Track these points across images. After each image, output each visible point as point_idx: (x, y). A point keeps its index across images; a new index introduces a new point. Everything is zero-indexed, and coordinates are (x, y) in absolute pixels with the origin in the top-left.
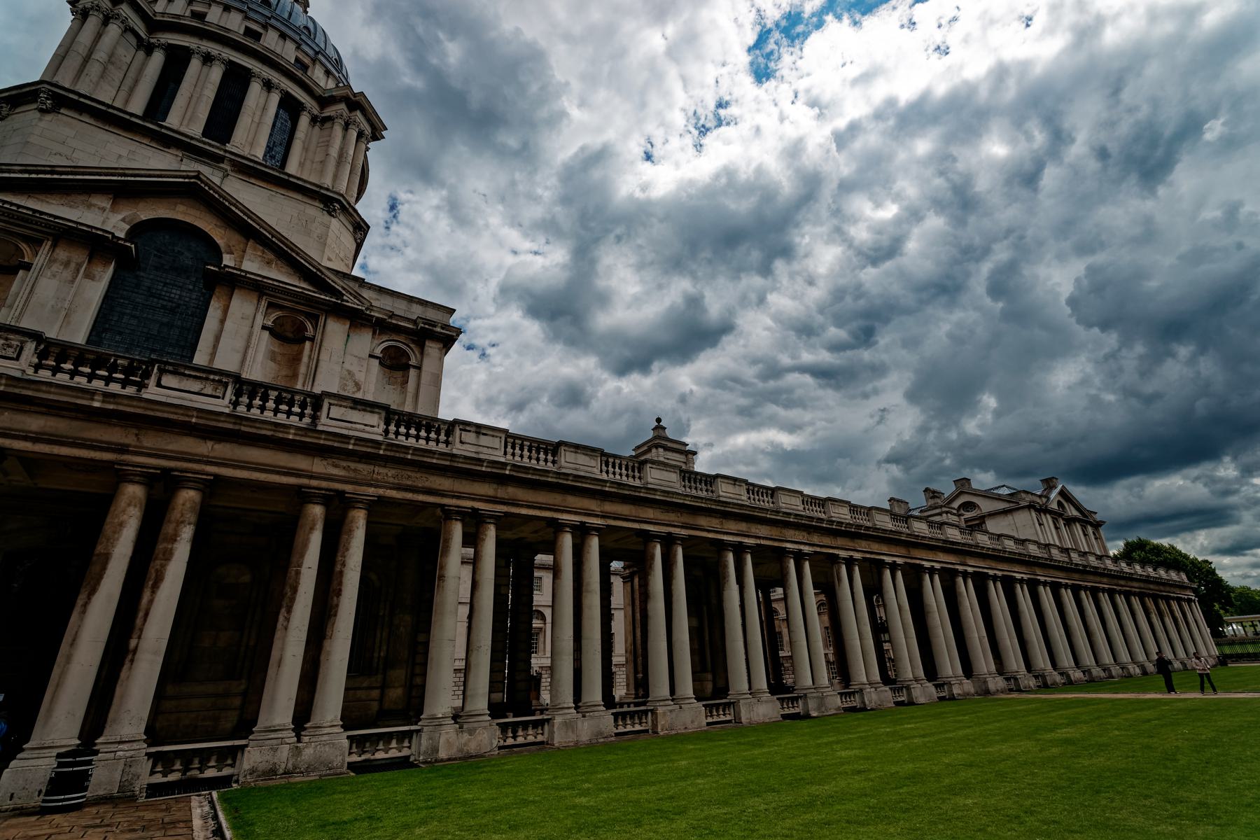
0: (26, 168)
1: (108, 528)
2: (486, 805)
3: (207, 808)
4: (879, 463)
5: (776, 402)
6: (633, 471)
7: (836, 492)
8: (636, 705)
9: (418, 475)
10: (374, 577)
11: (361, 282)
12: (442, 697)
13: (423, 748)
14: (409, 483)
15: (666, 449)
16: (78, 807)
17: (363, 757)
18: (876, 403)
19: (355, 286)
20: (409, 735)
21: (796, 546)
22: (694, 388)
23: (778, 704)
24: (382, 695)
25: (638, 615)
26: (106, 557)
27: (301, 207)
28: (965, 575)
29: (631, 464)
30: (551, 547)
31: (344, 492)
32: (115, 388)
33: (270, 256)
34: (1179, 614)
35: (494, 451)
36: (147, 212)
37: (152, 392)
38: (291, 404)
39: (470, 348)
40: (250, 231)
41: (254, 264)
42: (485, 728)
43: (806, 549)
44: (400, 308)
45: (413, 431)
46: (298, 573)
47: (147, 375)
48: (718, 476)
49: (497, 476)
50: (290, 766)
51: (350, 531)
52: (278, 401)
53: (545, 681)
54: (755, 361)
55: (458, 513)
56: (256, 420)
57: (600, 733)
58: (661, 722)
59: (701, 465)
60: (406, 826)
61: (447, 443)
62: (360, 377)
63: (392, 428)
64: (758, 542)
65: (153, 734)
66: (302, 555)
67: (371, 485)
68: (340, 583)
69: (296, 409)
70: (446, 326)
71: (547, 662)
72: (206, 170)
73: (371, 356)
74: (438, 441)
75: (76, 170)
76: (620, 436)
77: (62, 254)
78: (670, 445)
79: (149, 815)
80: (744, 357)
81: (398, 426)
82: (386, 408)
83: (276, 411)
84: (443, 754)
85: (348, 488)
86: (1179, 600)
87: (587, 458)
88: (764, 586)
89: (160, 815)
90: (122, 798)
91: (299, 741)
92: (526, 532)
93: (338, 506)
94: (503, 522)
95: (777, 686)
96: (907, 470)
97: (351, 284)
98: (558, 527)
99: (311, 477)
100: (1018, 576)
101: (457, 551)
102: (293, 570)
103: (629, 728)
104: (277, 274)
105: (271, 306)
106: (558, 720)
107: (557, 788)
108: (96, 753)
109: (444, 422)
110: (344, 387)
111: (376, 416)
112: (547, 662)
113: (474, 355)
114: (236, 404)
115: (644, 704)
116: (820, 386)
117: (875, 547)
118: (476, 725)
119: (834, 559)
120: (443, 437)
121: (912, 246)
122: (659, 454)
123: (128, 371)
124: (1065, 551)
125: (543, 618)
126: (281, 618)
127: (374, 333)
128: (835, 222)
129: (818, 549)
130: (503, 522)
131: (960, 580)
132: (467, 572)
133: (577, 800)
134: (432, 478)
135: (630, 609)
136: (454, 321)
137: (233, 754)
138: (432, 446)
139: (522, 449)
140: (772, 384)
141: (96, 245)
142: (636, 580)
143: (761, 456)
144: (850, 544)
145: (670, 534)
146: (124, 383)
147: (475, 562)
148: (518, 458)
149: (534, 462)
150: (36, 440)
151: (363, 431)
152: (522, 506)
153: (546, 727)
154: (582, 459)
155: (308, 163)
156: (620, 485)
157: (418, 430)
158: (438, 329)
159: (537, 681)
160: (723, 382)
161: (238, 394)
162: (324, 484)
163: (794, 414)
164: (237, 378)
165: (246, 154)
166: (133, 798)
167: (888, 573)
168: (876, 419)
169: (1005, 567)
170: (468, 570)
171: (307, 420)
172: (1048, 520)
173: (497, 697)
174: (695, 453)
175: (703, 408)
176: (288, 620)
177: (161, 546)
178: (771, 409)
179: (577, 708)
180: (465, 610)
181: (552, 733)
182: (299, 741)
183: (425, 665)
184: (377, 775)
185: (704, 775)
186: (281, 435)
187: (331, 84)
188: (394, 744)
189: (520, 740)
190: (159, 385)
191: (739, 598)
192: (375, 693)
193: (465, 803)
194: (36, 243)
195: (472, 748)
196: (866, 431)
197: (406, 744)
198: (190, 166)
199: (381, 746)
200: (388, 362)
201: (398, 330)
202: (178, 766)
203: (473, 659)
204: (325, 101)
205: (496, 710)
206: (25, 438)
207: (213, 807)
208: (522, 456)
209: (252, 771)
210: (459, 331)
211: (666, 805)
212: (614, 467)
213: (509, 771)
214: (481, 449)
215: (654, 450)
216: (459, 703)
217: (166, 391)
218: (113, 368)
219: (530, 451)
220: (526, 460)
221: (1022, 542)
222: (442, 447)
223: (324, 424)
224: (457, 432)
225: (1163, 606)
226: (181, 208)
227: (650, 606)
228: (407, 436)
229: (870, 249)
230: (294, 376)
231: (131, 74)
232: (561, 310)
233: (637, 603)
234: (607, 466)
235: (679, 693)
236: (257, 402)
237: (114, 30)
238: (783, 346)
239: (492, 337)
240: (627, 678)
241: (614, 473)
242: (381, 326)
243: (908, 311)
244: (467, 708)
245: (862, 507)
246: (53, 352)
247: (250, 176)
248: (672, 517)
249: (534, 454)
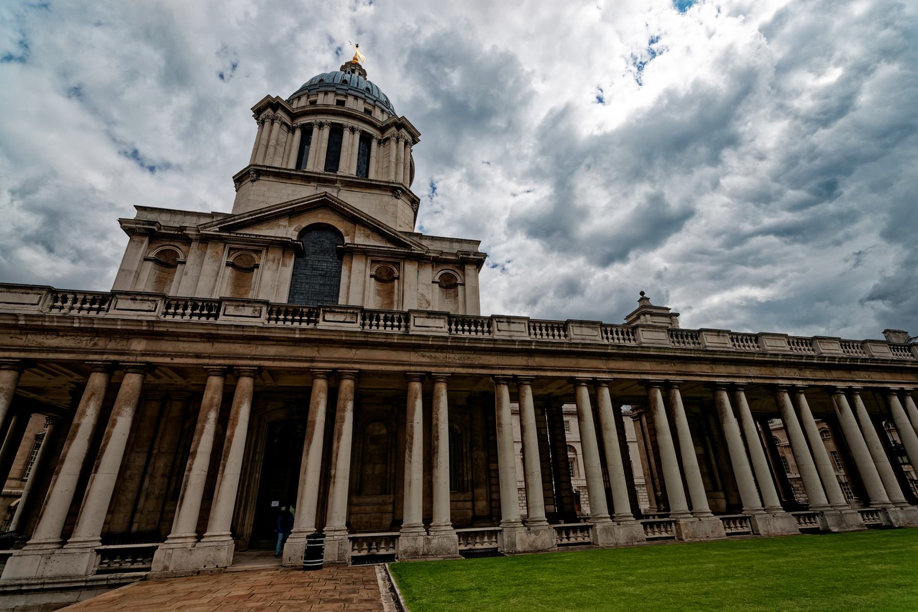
0: (251, 214)
1: (311, 406)
2: (556, 586)
3: (384, 574)
4: (861, 302)
5: (744, 264)
6: (628, 335)
7: (821, 331)
8: (660, 517)
9: (474, 356)
10: (456, 427)
12: (513, 509)
13: (505, 543)
14: (469, 362)
15: (652, 314)
16: (320, 568)
17: (468, 547)
18: (849, 248)
19: (416, 239)
20: (495, 533)
21: (789, 382)
22: (667, 265)
23: (795, 520)
24: (473, 505)
25: (650, 446)
26: (314, 422)
27: (380, 197)
29: (625, 330)
30: (573, 398)
31: (431, 373)
32: (304, 325)
33: (368, 232)
35: (521, 333)
37: (322, 325)
38: (392, 321)
39: (494, 266)
40: (356, 219)
41: (360, 239)
42: (545, 530)
43: (800, 384)
44: (446, 247)
45: (466, 327)
46: (412, 427)
47: (317, 316)
48: (701, 330)
49: (526, 350)
50: (425, 550)
51: (438, 397)
52: (385, 320)
53: (584, 497)
54: (717, 234)
55: (504, 379)
56: (375, 333)
57: (633, 538)
58: (684, 532)
59: (684, 323)
60: (504, 597)
61: (489, 332)
62: (429, 297)
63: (453, 327)
64: (750, 381)
65: (351, 527)
66: (413, 415)
67: (446, 366)
68: (437, 432)
69: (396, 323)
70: (476, 254)
71: (584, 483)
72: (328, 190)
73: (433, 282)
74: (483, 332)
75: (270, 208)
76: (613, 311)
77: (271, 256)
78: (654, 311)
79: (355, 575)
80: (707, 233)
81: (456, 325)
82: (448, 314)
83: (385, 326)
84: (519, 548)
85: (433, 369)
87: (590, 330)
88: (761, 418)
89: (361, 576)
90: (339, 564)
91: (428, 534)
92: (552, 389)
93: (428, 381)
94: (536, 383)
95: (789, 504)
96: (896, 303)
97: (415, 238)
98: (576, 383)
99: (411, 365)
101: (507, 407)
102: (408, 425)
103: (657, 535)
104: (373, 242)
105: (373, 261)
106: (599, 527)
107: (607, 578)
108: (324, 536)
109: (485, 318)
110: (420, 305)
111: (442, 321)
112: (584, 483)
113: (497, 270)
114: (363, 325)
115: (667, 516)
116: (786, 243)
117: (876, 376)
118: (539, 528)
119: (832, 391)
120: (486, 329)
121: (864, 99)
122: (647, 320)
123: (309, 314)
125: (575, 451)
126: (407, 455)
127: (433, 267)
128: (778, 100)
129: (813, 383)
130: (536, 383)
132: (515, 420)
133: (625, 589)
134: (484, 357)
135: (642, 442)
136: (481, 249)
137: (392, 541)
138: (480, 335)
139: (541, 330)
140: (737, 249)
141: (284, 246)
142: (644, 419)
143: (736, 311)
144: (847, 376)
145: (667, 381)
146: (308, 322)
147: (520, 413)
148: (539, 337)
149: (551, 337)
150: (274, 360)
151: (436, 331)
152: (547, 370)
153: (590, 531)
154: (586, 331)
155: (380, 171)
156: (619, 347)
157: (470, 326)
158: (472, 257)
159: (577, 497)
160: (689, 257)
161: (364, 319)
162: (418, 369)
163: (764, 271)
164: (362, 310)
165: (347, 175)
166: (345, 564)
167: (896, 400)
168: (852, 262)
170: (517, 417)
171: (403, 329)
173: (551, 508)
174: (677, 315)
175: (677, 279)
176: (410, 456)
177: (338, 414)
178: (741, 270)
179: (612, 518)
180: (519, 446)
181: (595, 536)
182: (428, 534)
183: (498, 485)
184: (479, 560)
185: (734, 577)
186: (390, 341)
187: (385, 117)
188: (486, 539)
189: (572, 540)
190: (324, 320)
191: (739, 430)
192: (469, 504)
193: (541, 584)
194: (258, 252)
195: (539, 544)
196: (843, 274)
197: (494, 539)
198: (322, 190)
199: (478, 540)
200: (444, 285)
201: (447, 262)
202: (365, 546)
203: (529, 481)
204: (383, 130)
205: (551, 518)
206: (269, 359)
207: (387, 574)
208: (541, 335)
209: (405, 552)
210: (485, 255)
211: (704, 600)
212: (612, 334)
213: (568, 563)
214: (512, 333)
215: (642, 317)
216: (525, 512)
217: (328, 323)
218: (301, 316)
219: (547, 330)
220: (545, 337)
222: (486, 336)
223: (413, 330)
224: (495, 324)
226: (320, 216)
227: (659, 439)
228: (463, 330)
229: (818, 114)
230: (392, 303)
231: (287, 148)
232: (553, 229)
233: (648, 436)
234: (606, 333)
235: (696, 508)
236: (374, 322)
237: (276, 125)
238: (743, 216)
239: (507, 256)
240: (649, 495)
241: (613, 339)
242: (437, 262)
243: (874, 158)
244: (531, 516)
245: (854, 342)
246: (275, 310)
247: (351, 186)
248: (666, 367)
249: (550, 332)
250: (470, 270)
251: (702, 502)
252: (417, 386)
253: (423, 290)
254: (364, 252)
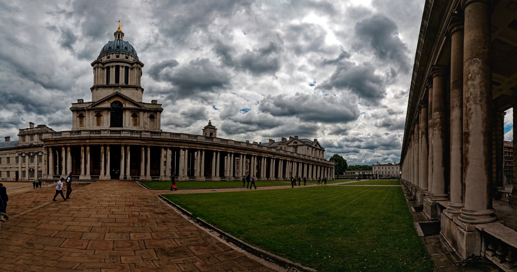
11: (144, 103)
36: (112, 101)
250: (158, 114)
251: (203, 174)
252: (143, 148)
253: (145, 120)
254: (129, 109)
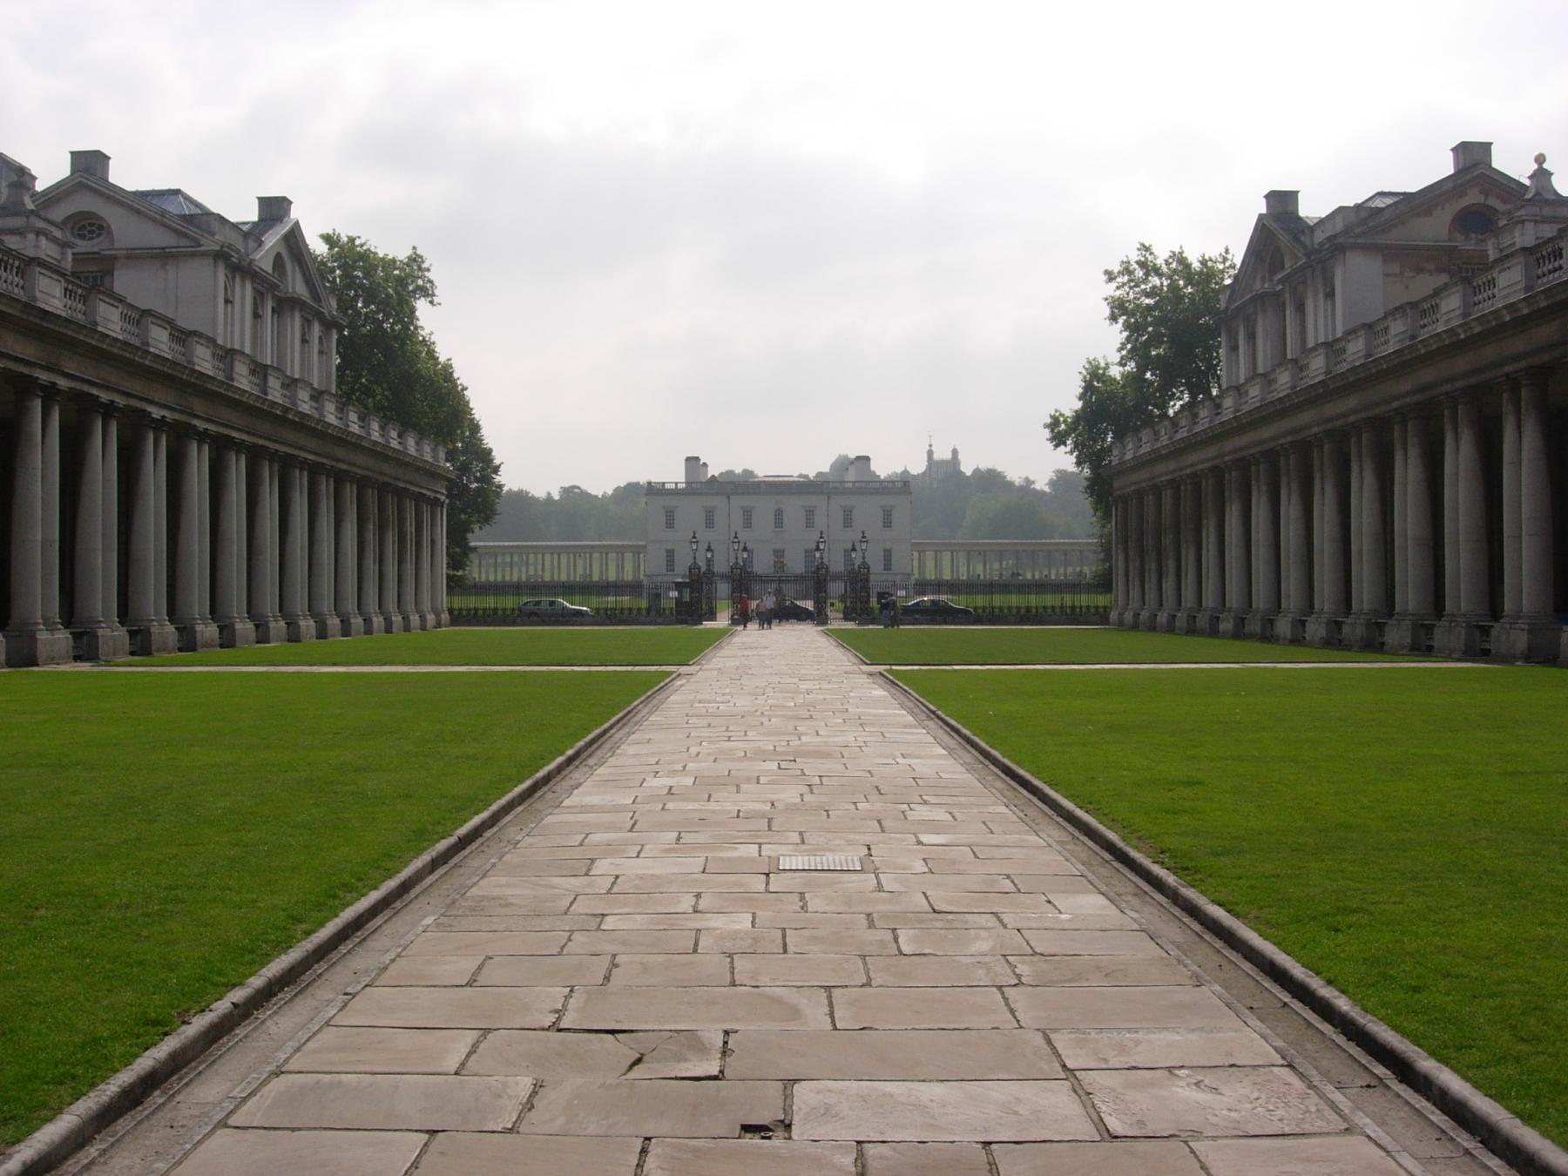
28: (50, 394)
34: (410, 528)
86: (419, 499)
100: (157, 413)
124: (260, 371)
131: (37, 405)
169: (137, 387)
172: (245, 293)
221: (182, 336)
225: (391, 509)
